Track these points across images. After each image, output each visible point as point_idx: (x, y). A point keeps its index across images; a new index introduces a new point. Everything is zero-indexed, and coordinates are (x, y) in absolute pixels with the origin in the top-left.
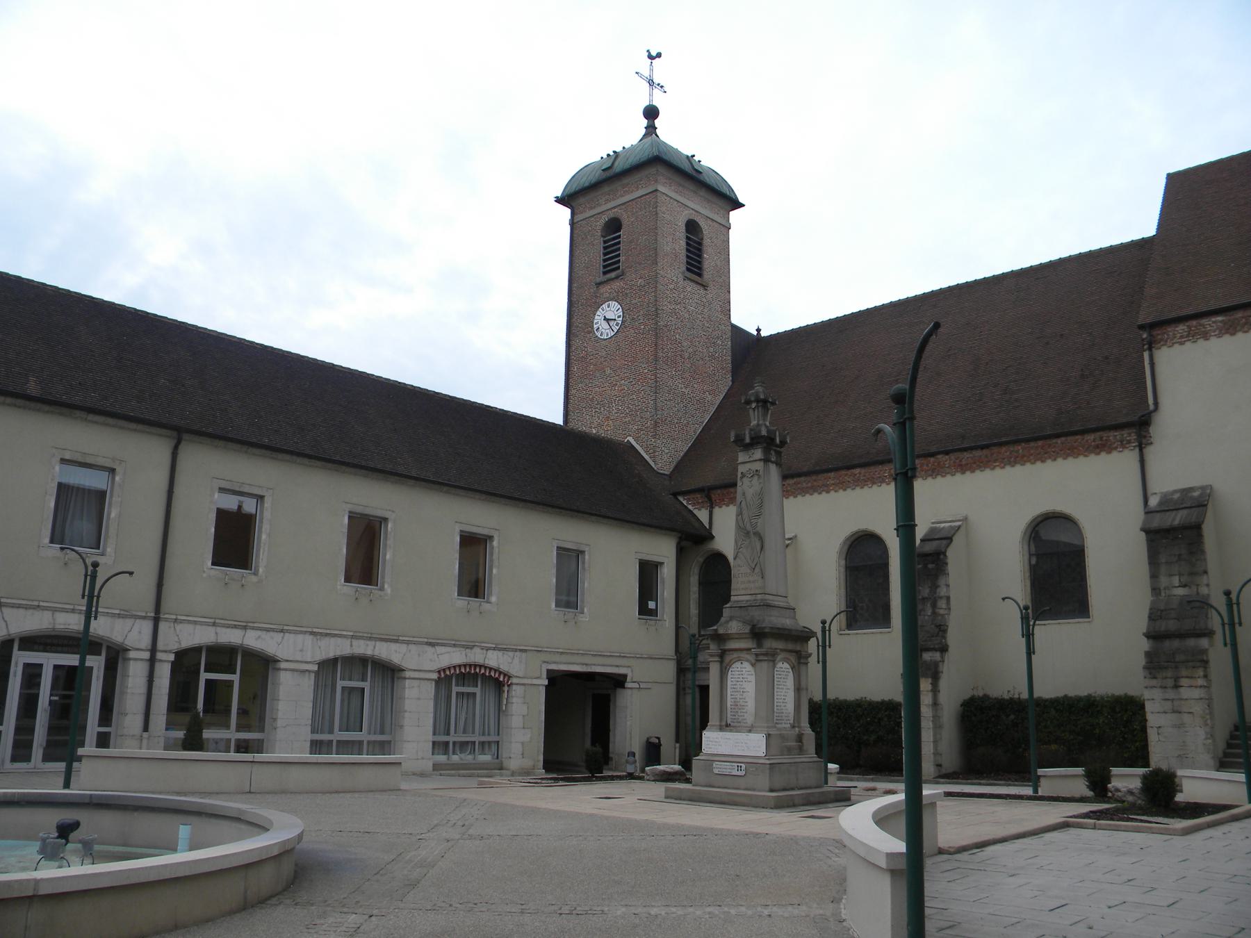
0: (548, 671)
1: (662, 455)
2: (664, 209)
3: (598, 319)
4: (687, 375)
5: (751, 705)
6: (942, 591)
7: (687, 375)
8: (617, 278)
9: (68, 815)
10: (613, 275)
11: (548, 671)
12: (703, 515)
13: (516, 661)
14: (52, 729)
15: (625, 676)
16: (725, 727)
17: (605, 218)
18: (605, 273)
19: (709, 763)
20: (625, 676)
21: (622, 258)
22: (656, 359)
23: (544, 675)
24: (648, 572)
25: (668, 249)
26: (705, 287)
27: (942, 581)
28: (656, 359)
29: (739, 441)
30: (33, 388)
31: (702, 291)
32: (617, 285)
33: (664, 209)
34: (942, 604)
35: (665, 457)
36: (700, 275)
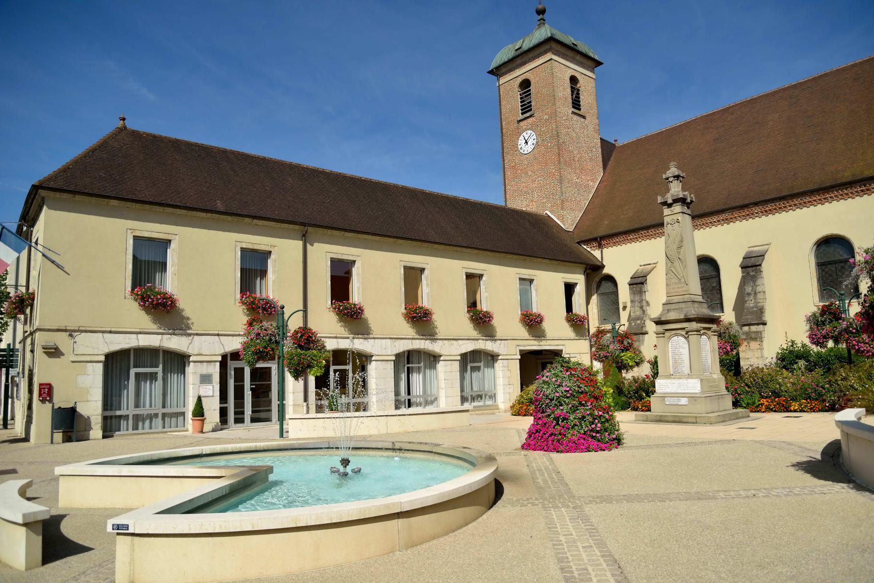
0: (520, 351)
1: (567, 220)
2: (556, 70)
3: (521, 141)
4: (578, 171)
5: (709, 361)
6: (759, 289)
7: (578, 171)
8: (531, 116)
9: (344, 454)
10: (528, 114)
11: (520, 351)
12: (597, 253)
13: (502, 345)
14: (254, 405)
15: (562, 351)
16: (669, 376)
17: (520, 80)
18: (522, 114)
19: (663, 397)
20: (562, 351)
21: (533, 104)
22: (560, 163)
23: (518, 353)
24: (569, 289)
25: (560, 95)
26: (584, 117)
27: (759, 282)
28: (560, 163)
29: (665, 203)
30: (220, 206)
31: (583, 120)
32: (530, 120)
33: (556, 70)
34: (760, 296)
35: (569, 221)
36: (580, 110)
